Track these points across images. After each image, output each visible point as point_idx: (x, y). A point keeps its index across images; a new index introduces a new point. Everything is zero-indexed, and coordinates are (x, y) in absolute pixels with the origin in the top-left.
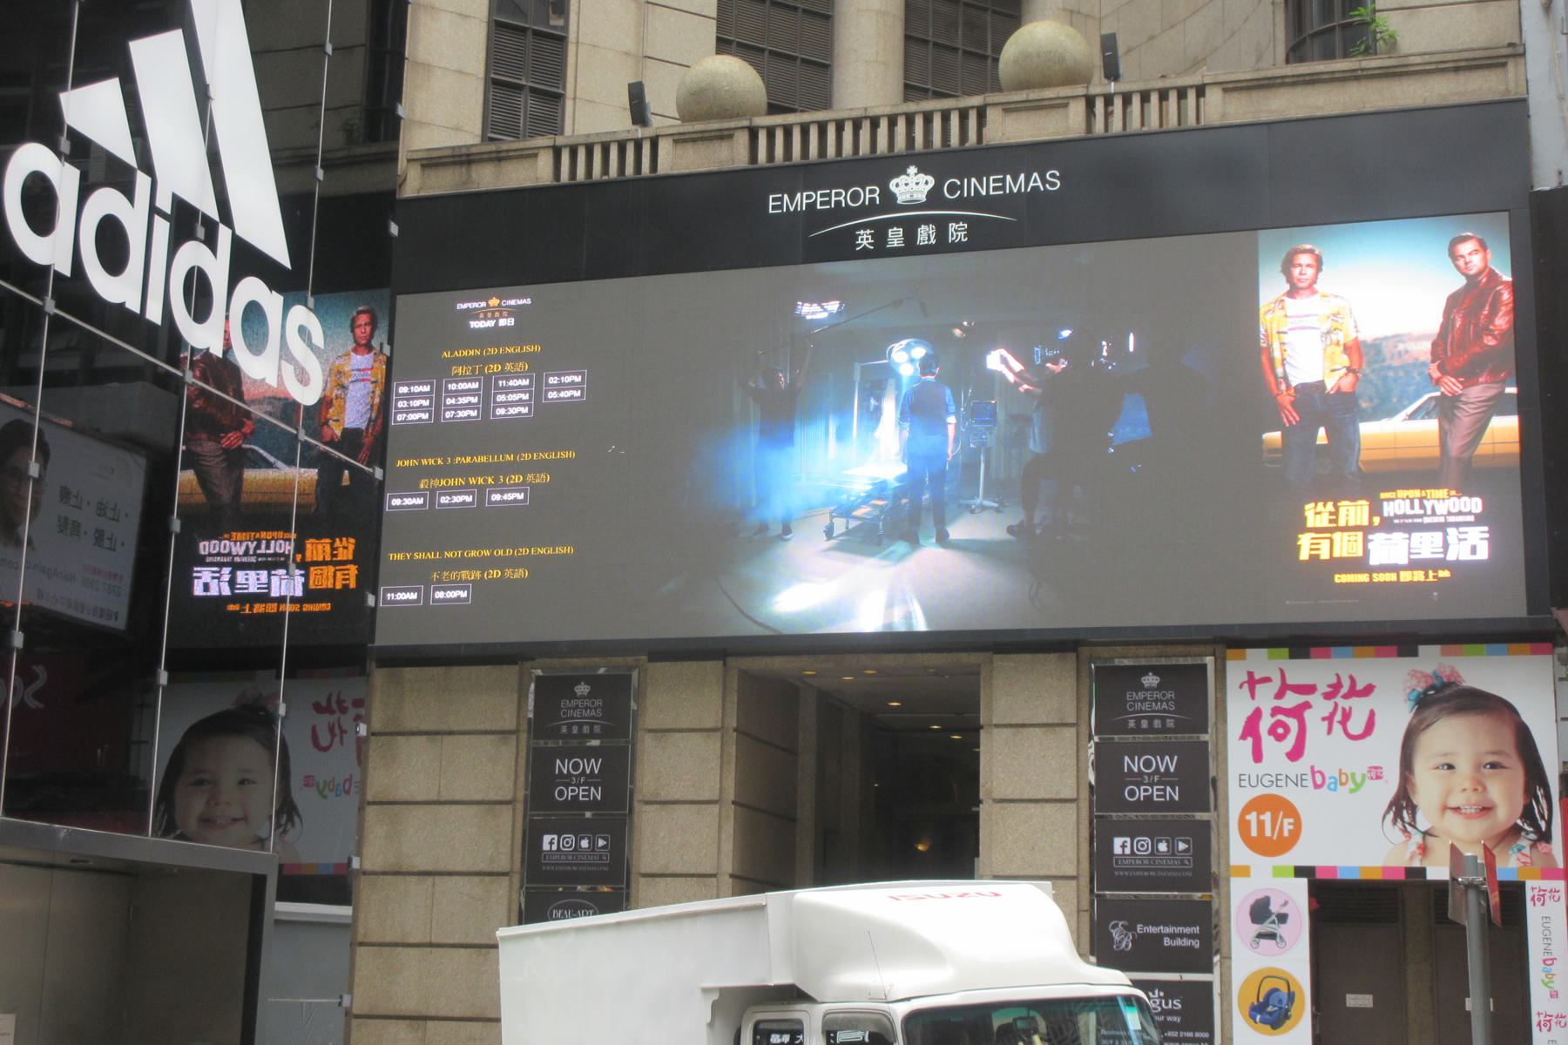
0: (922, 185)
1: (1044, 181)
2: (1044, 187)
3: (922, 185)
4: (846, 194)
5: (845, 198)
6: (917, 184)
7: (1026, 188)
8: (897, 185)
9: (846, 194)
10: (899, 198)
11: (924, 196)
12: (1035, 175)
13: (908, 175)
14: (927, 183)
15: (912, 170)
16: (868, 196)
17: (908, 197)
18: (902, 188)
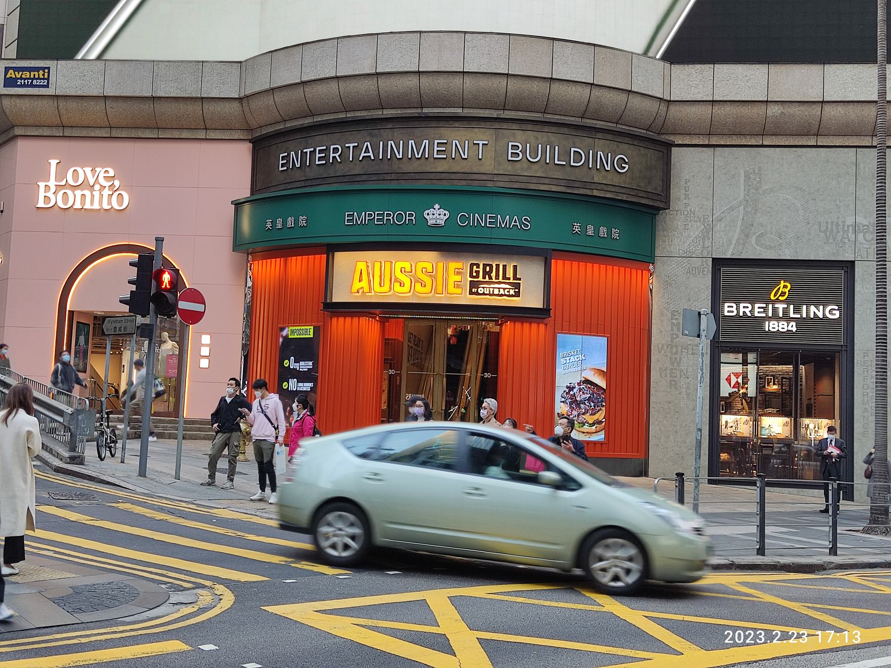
0: (442, 216)
1: (521, 223)
2: (521, 226)
3: (442, 216)
4: (394, 216)
5: (393, 218)
6: (440, 215)
7: (510, 226)
8: (428, 214)
9: (394, 216)
10: (429, 222)
11: (443, 223)
12: (516, 217)
13: (435, 209)
14: (445, 215)
15: (437, 206)
16: (407, 218)
17: (434, 222)
18: (431, 216)
